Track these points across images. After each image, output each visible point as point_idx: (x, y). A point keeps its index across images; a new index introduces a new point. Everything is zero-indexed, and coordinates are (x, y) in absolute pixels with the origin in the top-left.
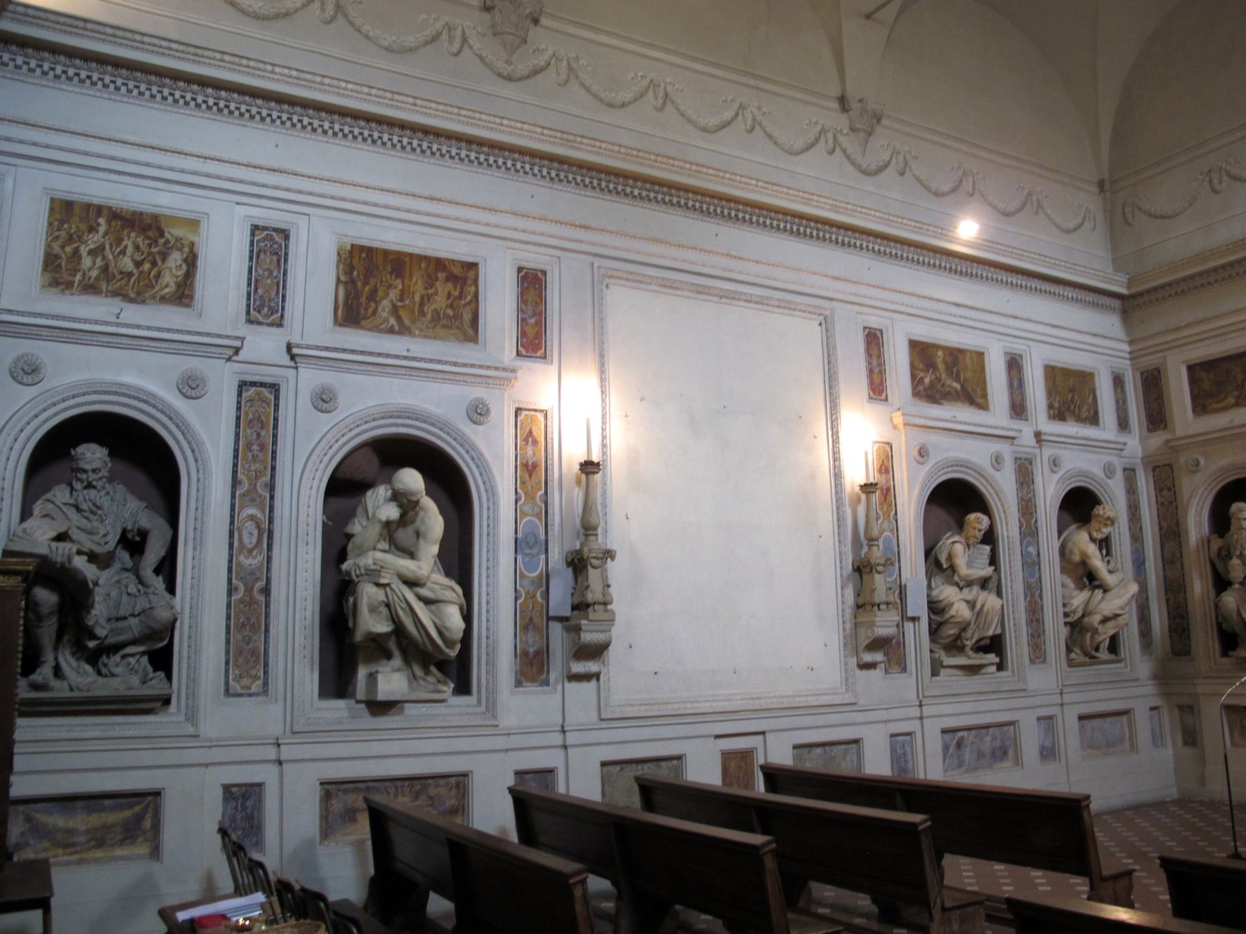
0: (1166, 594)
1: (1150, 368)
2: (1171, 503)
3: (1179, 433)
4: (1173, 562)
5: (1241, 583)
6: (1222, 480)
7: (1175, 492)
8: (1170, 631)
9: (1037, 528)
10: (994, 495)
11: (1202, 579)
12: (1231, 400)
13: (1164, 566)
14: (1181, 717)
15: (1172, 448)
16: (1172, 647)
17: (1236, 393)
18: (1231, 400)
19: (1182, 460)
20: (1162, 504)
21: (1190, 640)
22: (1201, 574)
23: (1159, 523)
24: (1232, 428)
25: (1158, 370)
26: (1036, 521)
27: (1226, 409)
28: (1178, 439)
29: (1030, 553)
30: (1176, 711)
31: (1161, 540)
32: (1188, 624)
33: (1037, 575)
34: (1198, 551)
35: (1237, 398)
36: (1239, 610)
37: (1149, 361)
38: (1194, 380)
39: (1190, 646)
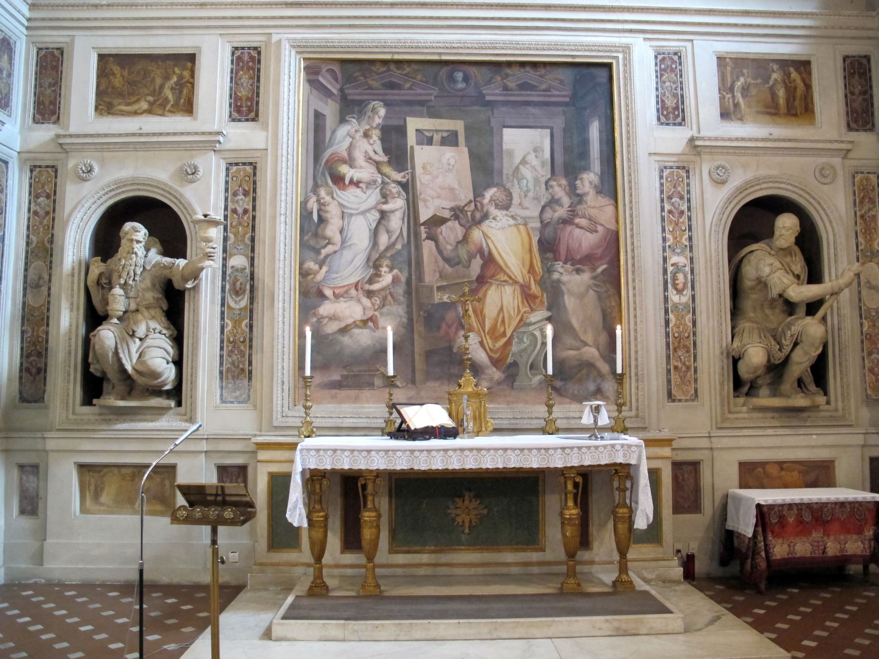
0: (23, 324)
1: (51, 46)
2: (47, 213)
3: (73, 130)
4: (37, 286)
5: (119, 319)
6: (116, 195)
7: (55, 201)
8: (21, 371)
11: (71, 310)
12: (144, 105)
13: (25, 289)
14: (21, 479)
15: (62, 146)
16: (21, 392)
17: (151, 98)
18: (144, 105)
19: (71, 164)
20: (36, 213)
21: (45, 385)
22: (72, 304)
23: (28, 236)
24: (141, 135)
25: (61, 50)
27: (136, 113)
28: (71, 136)
30: (16, 472)
31: (26, 257)
32: (46, 365)
34: (73, 275)
35: (151, 104)
36: (116, 348)
37: (53, 38)
38: (103, 73)
39: (44, 391)
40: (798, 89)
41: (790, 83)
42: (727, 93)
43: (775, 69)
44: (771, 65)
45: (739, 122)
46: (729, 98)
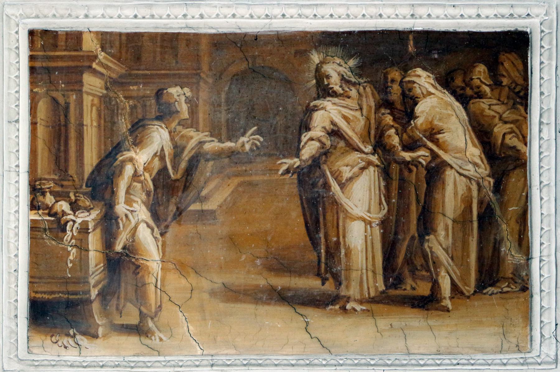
40: (450, 175)
41: (410, 146)
42: (75, 207)
43: (335, 83)
44: (316, 58)
45: (134, 340)
46: (84, 230)
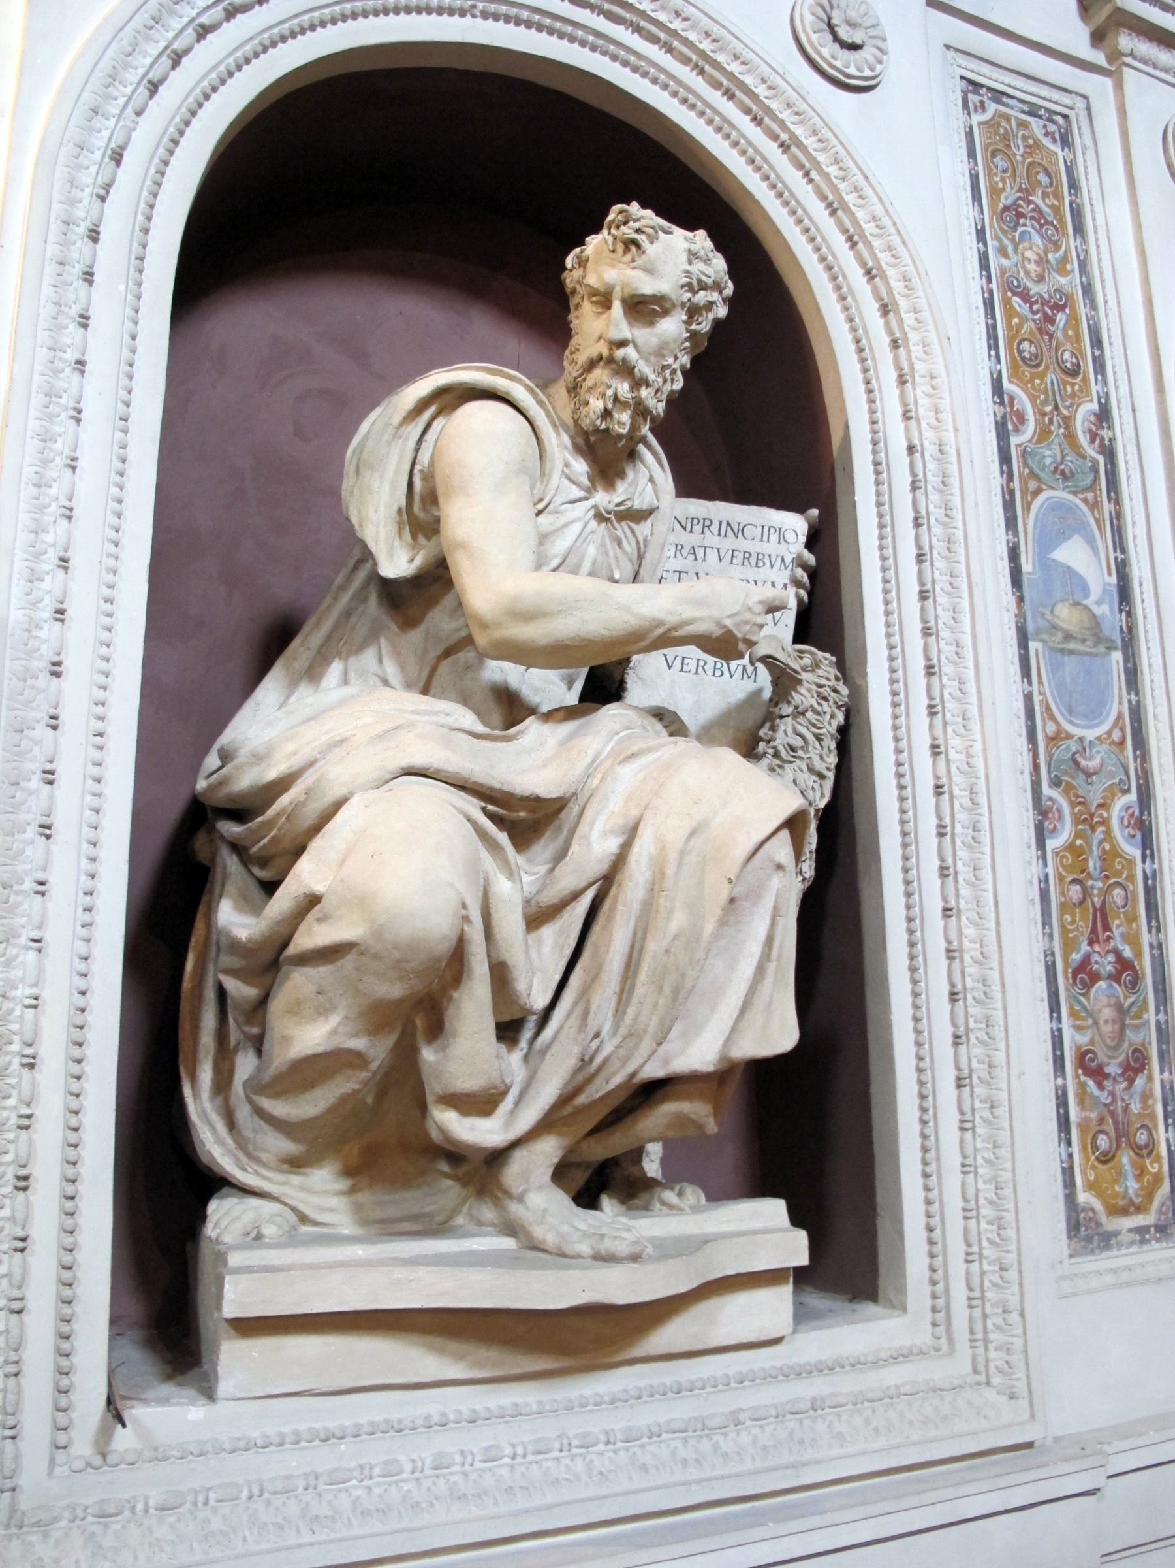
9: (1109, 453)
10: (818, 210)
26: (1104, 415)
29: (1074, 581)
33: (1118, 703)
